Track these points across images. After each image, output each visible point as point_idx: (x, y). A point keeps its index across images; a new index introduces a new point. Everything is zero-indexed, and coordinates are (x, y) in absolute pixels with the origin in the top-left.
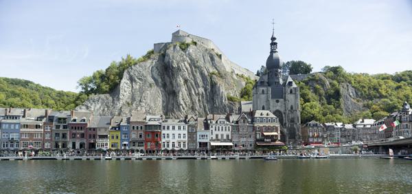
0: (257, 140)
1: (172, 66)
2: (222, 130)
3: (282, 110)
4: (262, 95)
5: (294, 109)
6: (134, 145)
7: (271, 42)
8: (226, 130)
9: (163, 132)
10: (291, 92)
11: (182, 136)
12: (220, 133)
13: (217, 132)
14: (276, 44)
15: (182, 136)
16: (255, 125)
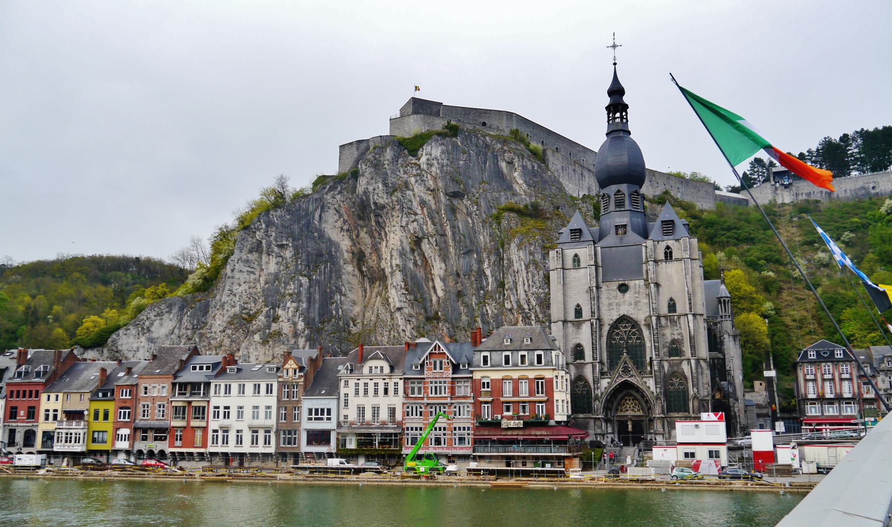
0: (484, 425)
1: (375, 204)
2: (376, 392)
3: (640, 315)
4: (572, 274)
5: (680, 309)
6: (145, 439)
7: (607, 100)
8: (386, 391)
9: (215, 401)
10: (669, 255)
11: (262, 411)
12: (369, 402)
13: (361, 400)
14: (625, 107)
15: (262, 411)
16: (477, 376)
